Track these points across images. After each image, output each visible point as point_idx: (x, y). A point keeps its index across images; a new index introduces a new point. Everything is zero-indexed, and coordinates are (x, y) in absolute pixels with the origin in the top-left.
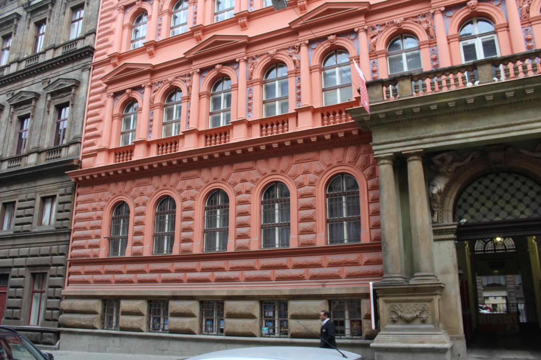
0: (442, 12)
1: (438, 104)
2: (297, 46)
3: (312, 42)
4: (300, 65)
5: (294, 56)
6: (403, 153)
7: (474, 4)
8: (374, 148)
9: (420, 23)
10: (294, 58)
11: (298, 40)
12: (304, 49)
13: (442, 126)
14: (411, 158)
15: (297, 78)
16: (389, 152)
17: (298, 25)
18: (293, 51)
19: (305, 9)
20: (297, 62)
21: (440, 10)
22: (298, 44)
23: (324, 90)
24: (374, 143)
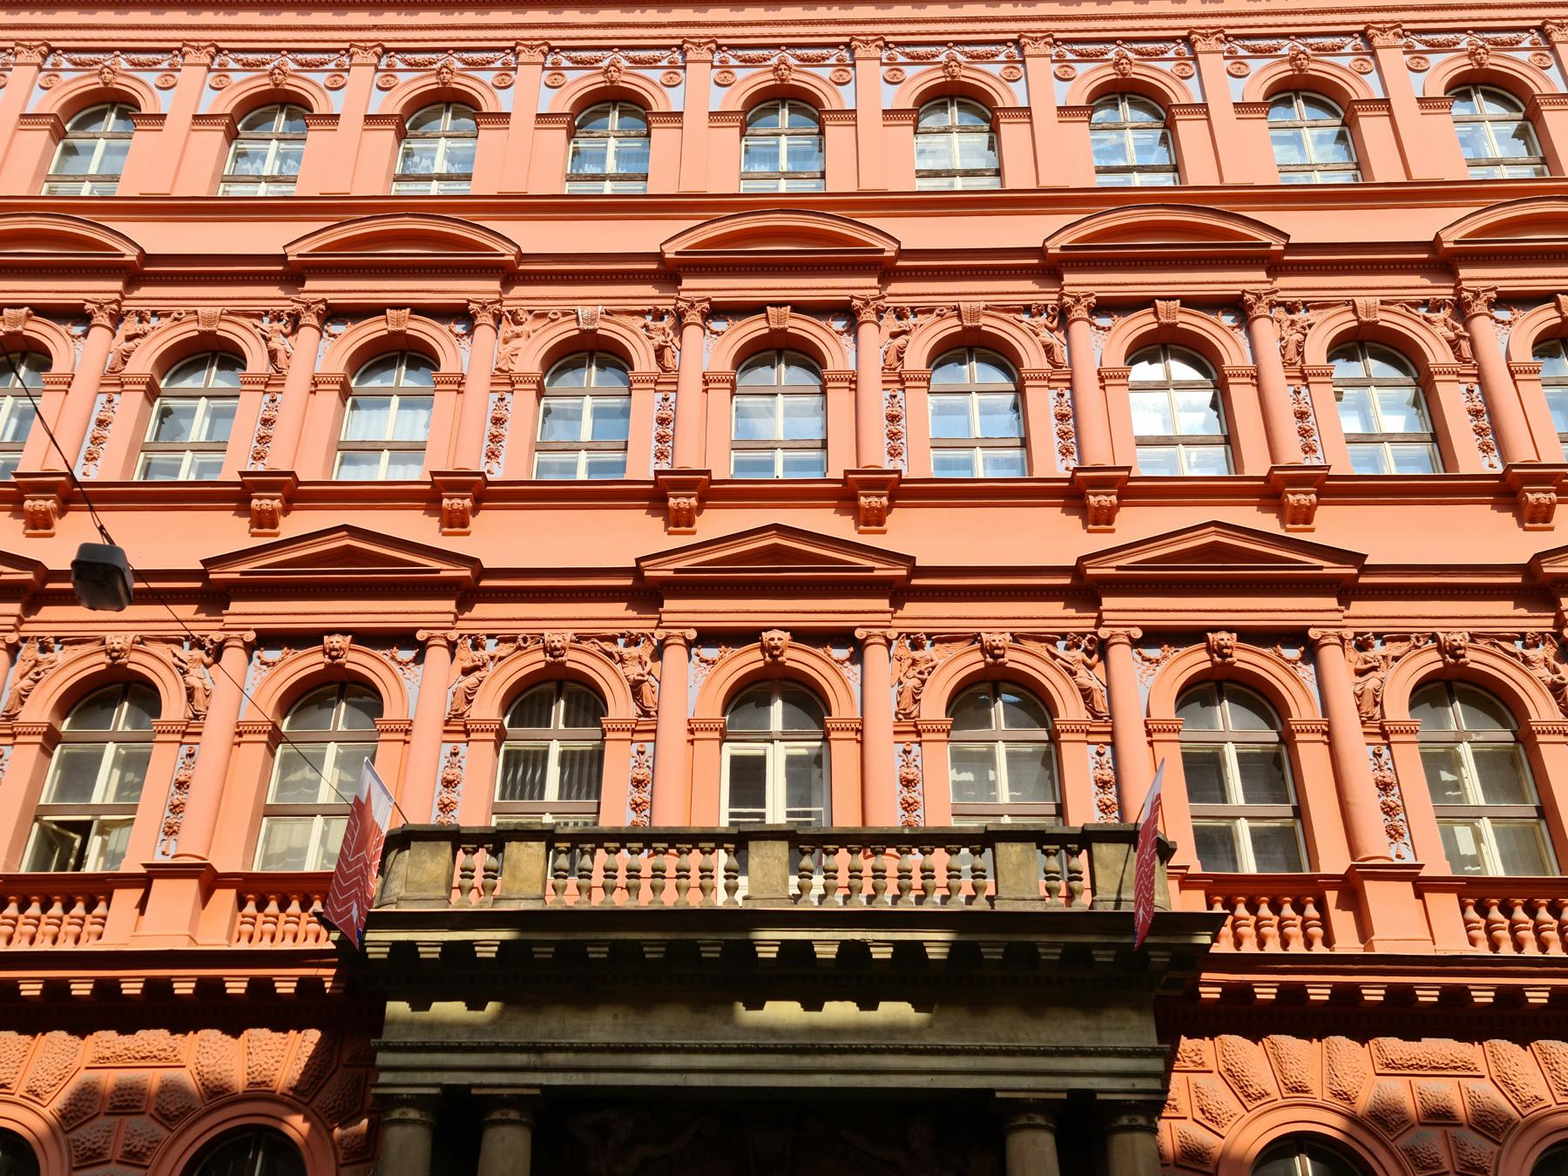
0: (689, 645)
1: (614, 944)
2: (212, 642)
3: (268, 639)
4: (207, 708)
5: (192, 671)
6: (474, 1091)
7: (779, 643)
8: (383, 1058)
9: (622, 660)
10: (192, 680)
11: (222, 621)
12: (233, 657)
13: (615, 1016)
14: (496, 1116)
15: (184, 750)
16: (428, 1083)
17: (232, 573)
18: (198, 654)
19: (274, 525)
20: (199, 695)
21: (684, 638)
22: (218, 637)
23: (272, 812)
24: (386, 1043)
